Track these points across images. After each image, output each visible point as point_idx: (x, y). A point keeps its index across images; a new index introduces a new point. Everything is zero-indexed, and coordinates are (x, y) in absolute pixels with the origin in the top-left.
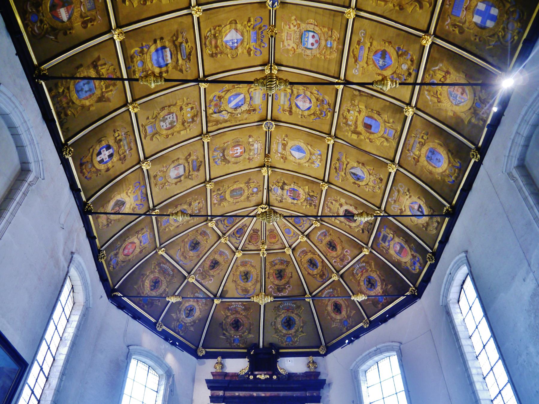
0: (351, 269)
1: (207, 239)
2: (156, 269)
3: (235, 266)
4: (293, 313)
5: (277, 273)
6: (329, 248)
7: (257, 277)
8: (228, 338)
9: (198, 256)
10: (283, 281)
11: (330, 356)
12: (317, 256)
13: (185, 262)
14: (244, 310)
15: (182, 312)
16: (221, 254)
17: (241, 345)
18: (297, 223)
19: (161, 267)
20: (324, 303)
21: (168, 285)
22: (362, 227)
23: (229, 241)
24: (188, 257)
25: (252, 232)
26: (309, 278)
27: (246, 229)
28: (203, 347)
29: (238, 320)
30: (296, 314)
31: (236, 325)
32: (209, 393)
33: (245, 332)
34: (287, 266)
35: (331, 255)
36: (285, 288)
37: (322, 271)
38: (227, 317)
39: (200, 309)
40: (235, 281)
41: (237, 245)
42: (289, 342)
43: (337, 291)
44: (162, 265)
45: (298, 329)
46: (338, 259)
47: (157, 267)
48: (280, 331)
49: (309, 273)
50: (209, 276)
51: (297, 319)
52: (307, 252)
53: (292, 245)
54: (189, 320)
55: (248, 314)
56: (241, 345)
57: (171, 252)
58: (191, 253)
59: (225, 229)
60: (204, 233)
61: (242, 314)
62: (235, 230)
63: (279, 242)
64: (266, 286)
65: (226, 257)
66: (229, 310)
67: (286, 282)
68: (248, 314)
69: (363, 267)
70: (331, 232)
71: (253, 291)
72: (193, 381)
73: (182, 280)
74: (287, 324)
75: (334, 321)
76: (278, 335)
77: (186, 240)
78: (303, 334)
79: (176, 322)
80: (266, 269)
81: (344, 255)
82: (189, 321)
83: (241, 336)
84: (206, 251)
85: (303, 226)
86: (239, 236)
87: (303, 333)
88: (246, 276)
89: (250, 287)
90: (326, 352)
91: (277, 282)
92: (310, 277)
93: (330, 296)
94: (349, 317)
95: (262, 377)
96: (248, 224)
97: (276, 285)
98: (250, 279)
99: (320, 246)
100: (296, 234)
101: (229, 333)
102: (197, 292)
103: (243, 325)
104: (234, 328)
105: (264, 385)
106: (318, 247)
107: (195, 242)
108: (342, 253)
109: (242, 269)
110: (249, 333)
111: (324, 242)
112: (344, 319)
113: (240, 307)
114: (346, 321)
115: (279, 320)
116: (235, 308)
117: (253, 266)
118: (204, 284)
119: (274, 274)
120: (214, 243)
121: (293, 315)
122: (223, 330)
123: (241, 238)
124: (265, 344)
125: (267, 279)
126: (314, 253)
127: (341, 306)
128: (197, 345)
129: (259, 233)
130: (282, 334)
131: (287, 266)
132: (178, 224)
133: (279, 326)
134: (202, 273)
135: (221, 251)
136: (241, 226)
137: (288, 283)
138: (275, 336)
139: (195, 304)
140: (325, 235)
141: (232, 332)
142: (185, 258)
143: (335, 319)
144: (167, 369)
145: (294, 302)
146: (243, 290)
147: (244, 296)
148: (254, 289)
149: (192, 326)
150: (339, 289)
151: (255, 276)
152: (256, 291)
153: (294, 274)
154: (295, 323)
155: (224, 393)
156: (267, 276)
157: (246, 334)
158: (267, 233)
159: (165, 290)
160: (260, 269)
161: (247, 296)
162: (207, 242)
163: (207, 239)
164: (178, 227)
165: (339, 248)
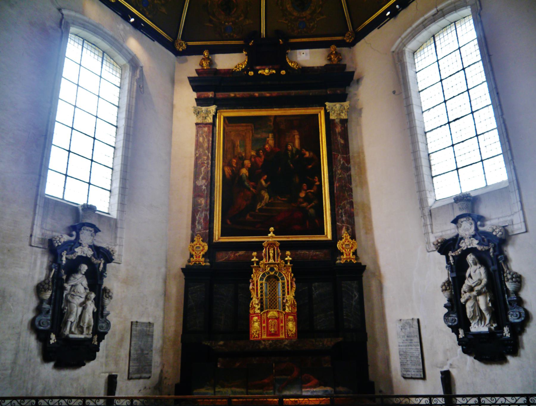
11: (359, 44)
28: (182, 39)
32: (194, 95)
72: (173, 82)
78: (322, 17)
95: (266, 72)
105: (269, 83)
155: (215, 95)
157: (241, 19)
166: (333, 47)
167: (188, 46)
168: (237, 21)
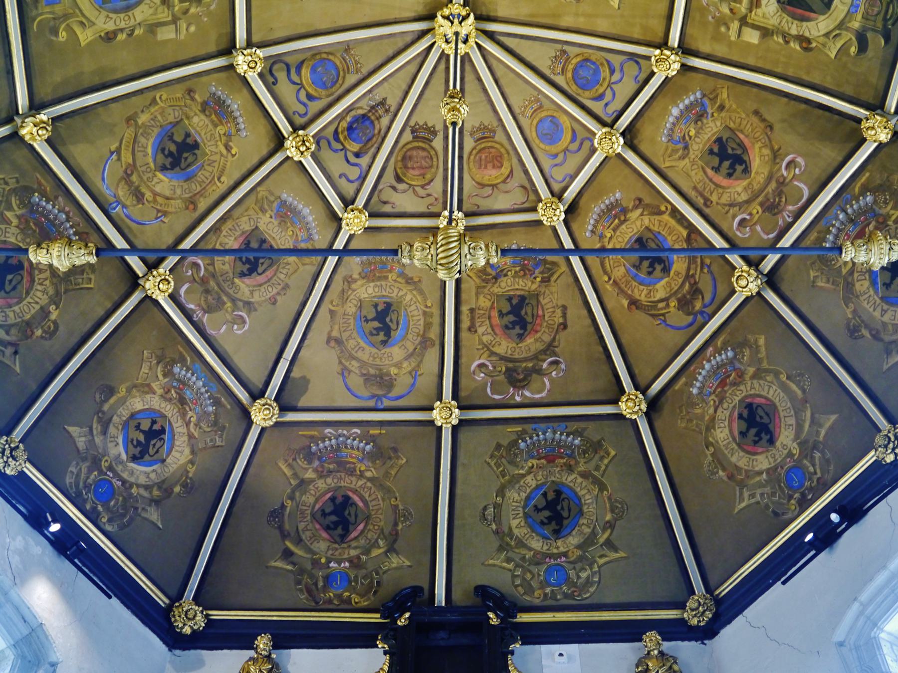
0: (813, 236)
1: (229, 136)
2: (10, 208)
3: (338, 277)
4: (570, 469)
5: (506, 308)
6: (716, 170)
7: (428, 326)
8: (302, 571)
9: (192, 202)
10: (529, 340)
11: (727, 633)
12: (666, 217)
13: (136, 211)
14: (372, 457)
15: (112, 430)
16: (286, 214)
17: (355, 598)
18: (583, 87)
19: (32, 209)
20: (701, 417)
21: (57, 293)
22: (856, 25)
23: (314, 156)
24: (148, 195)
25: (408, 136)
26: (639, 327)
27: (385, 121)
28: (197, 600)
29: (347, 498)
30: (585, 475)
31: (340, 516)
33: (375, 545)
34: (546, 281)
35: (725, 199)
36: (539, 372)
37: (688, 277)
38: (303, 484)
39: (191, 436)
40: (339, 341)
41: (349, 189)
42: (559, 585)
43: (756, 349)
44: (36, 198)
45: (594, 534)
46: (756, 208)
47: (14, 202)
48: (521, 543)
49: (634, 303)
50: (233, 301)
51: (586, 493)
52: (625, 211)
53: (565, 189)
54: (140, 473)
55: (387, 474)
56: (355, 598)
57: (81, 153)
58: (164, 183)
59: (302, 110)
60: (216, 108)
61: (362, 475)
62: (341, 117)
63: (513, 183)
64: (463, 360)
65: (302, 235)
66: (309, 456)
67: (540, 346)
68: (387, 474)
69: (862, 212)
70: (725, 95)
71: (409, 380)
73: (123, 288)
74: (547, 513)
75: (742, 485)
76: (508, 560)
77: (143, 118)
78: (614, 555)
79: (84, 467)
80: (464, 296)
81: (782, 183)
82: (142, 480)
83: (356, 563)
84: (222, 188)
85: (608, 96)
86: (354, 147)
87: (615, 549)
88: (383, 320)
89: (398, 365)
90: (716, 616)
91: (504, 346)
92: (640, 316)
93: (726, 378)
94: (808, 447)
96: (392, 102)
97: (502, 358)
98: (396, 334)
99: (680, 168)
100: (581, 134)
101: (309, 551)
102: (183, 360)
103: (368, 518)
104: (327, 528)
106: (671, 174)
107: (178, 138)
108: (769, 179)
109: (367, 291)
110: (391, 549)
111: (697, 147)
112: (789, 464)
113: (356, 448)
114: (797, 467)
115: (515, 496)
116: (338, 449)
117: (409, 281)
118: (211, 331)
119: (495, 313)
120: (255, 160)
121: (569, 479)
122: (284, 536)
123: (364, 161)
124: (457, 596)
125: (464, 335)
126: (654, 204)
127: (771, 409)
128: (173, 592)
129: (438, 143)
130: (529, 555)
131: (546, 281)
132: (110, 26)
133: (516, 524)
134: (204, 281)
135: (283, 203)
136: (365, 105)
137: (549, 349)
138: (499, 561)
139: (169, 410)
140: (700, 117)
141: (322, 546)
142: (139, 196)
143: (749, 474)
144: (25, 631)
145: (574, 426)
146: (368, 379)
147: (371, 403)
148: (414, 374)
149: (157, 502)
150: (762, 341)
151: (417, 322)
152: (420, 380)
153: (575, 313)
154: (581, 513)
156: (465, 323)
157: (375, 552)
158: (469, 143)
159: (44, 313)
160: (437, 294)
161: (387, 403)
162: (228, 148)
163: (229, 136)
164: (109, 37)
165: (758, 160)
166: (651, 638)
167: (210, 623)
168: (364, 558)
